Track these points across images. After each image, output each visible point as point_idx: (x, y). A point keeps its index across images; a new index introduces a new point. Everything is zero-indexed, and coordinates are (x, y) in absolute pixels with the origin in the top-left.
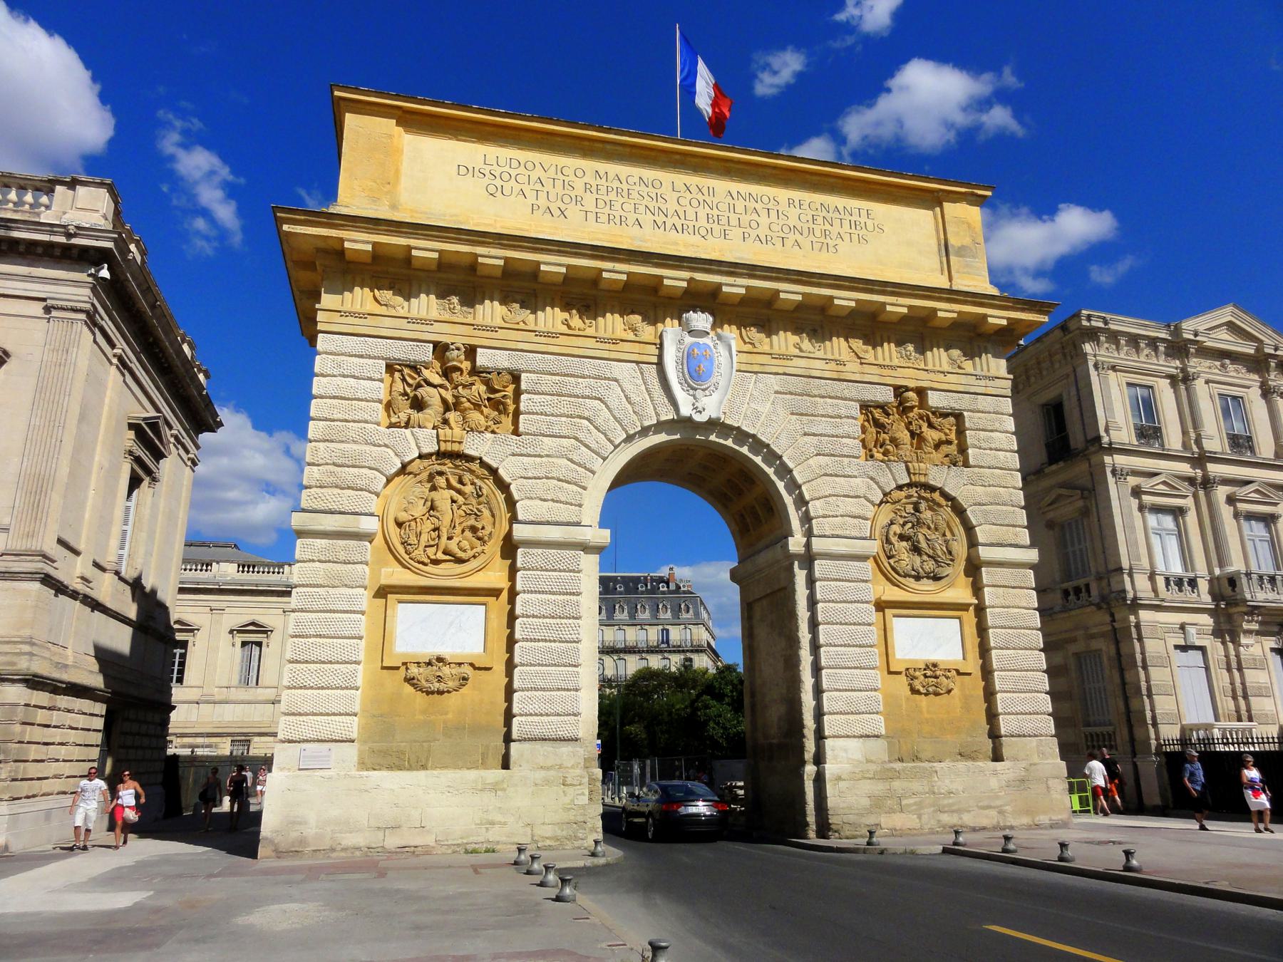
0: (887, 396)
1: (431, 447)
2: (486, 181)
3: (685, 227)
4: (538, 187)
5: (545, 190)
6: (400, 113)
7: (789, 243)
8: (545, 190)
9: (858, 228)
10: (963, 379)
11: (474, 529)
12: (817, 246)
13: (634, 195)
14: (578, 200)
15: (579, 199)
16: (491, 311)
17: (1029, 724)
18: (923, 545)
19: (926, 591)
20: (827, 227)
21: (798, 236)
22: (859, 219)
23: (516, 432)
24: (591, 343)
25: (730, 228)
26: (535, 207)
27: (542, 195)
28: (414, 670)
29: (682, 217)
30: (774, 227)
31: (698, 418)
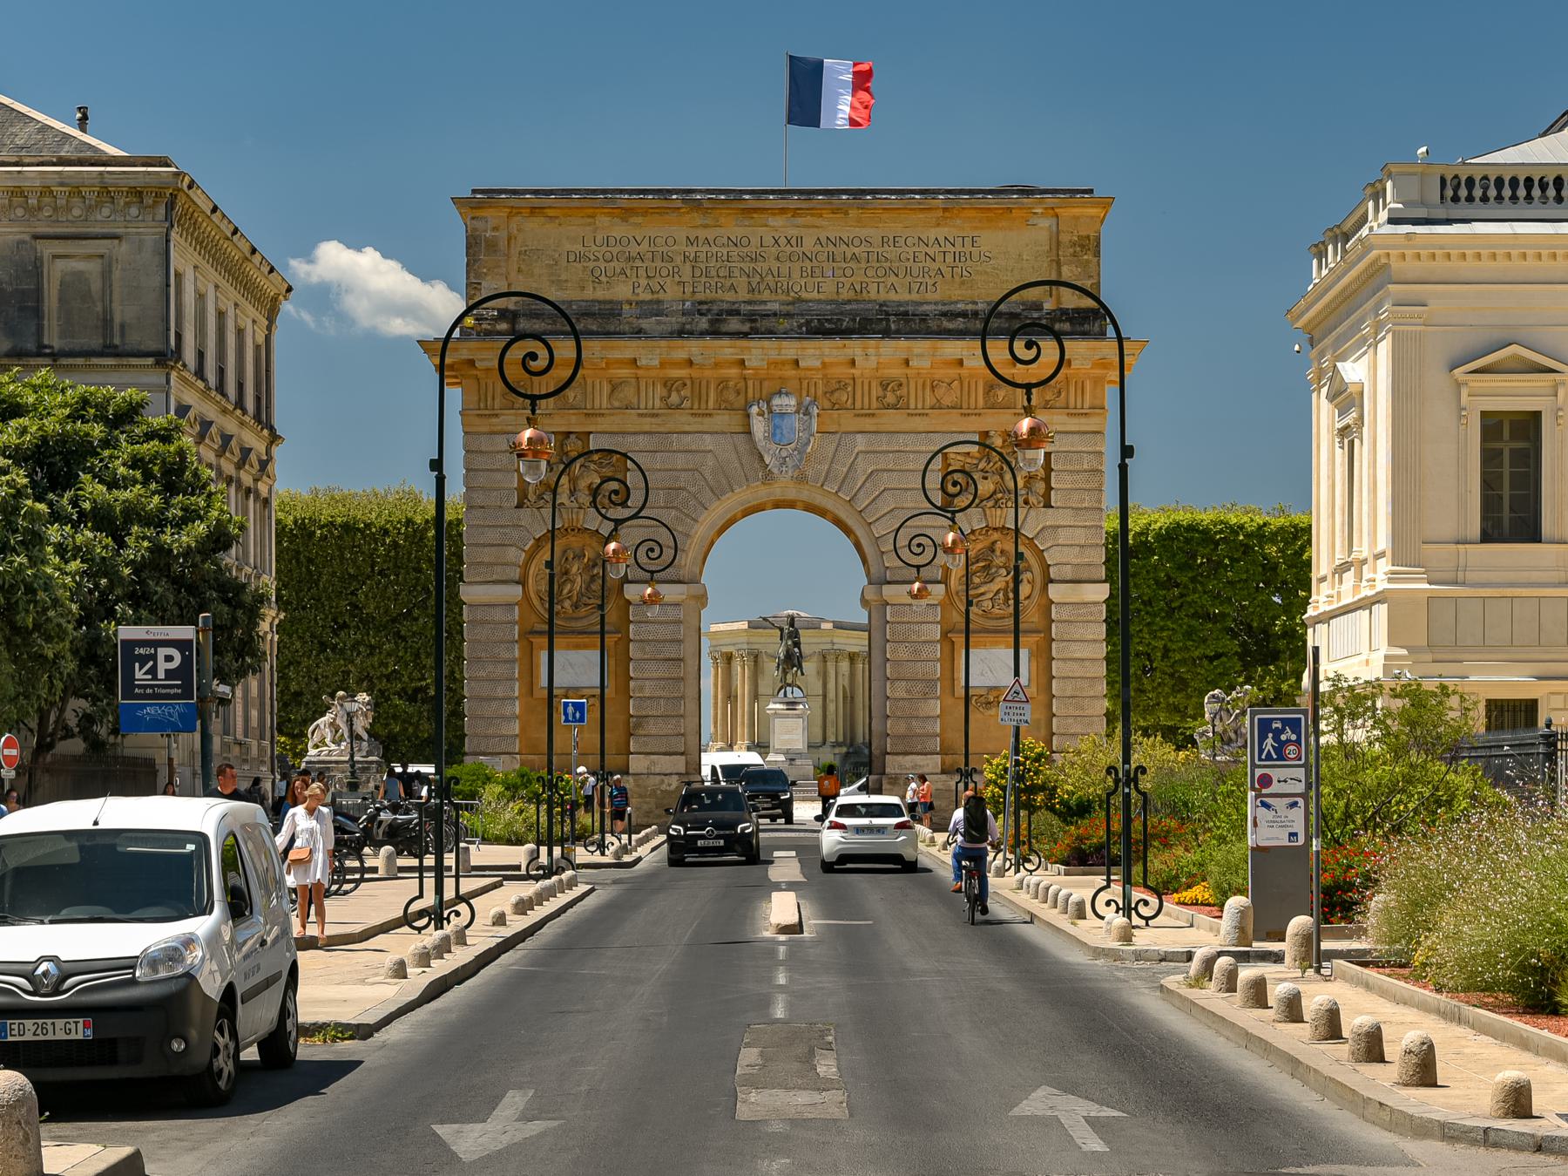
2: (591, 265)
3: (779, 284)
4: (638, 263)
5: (644, 265)
6: (508, 210)
8: (644, 265)
9: (963, 259)
12: (915, 287)
15: (676, 270)
20: (929, 262)
21: (893, 279)
22: (964, 249)
25: (823, 280)
26: (636, 285)
27: (642, 272)
29: (776, 274)
30: (870, 273)
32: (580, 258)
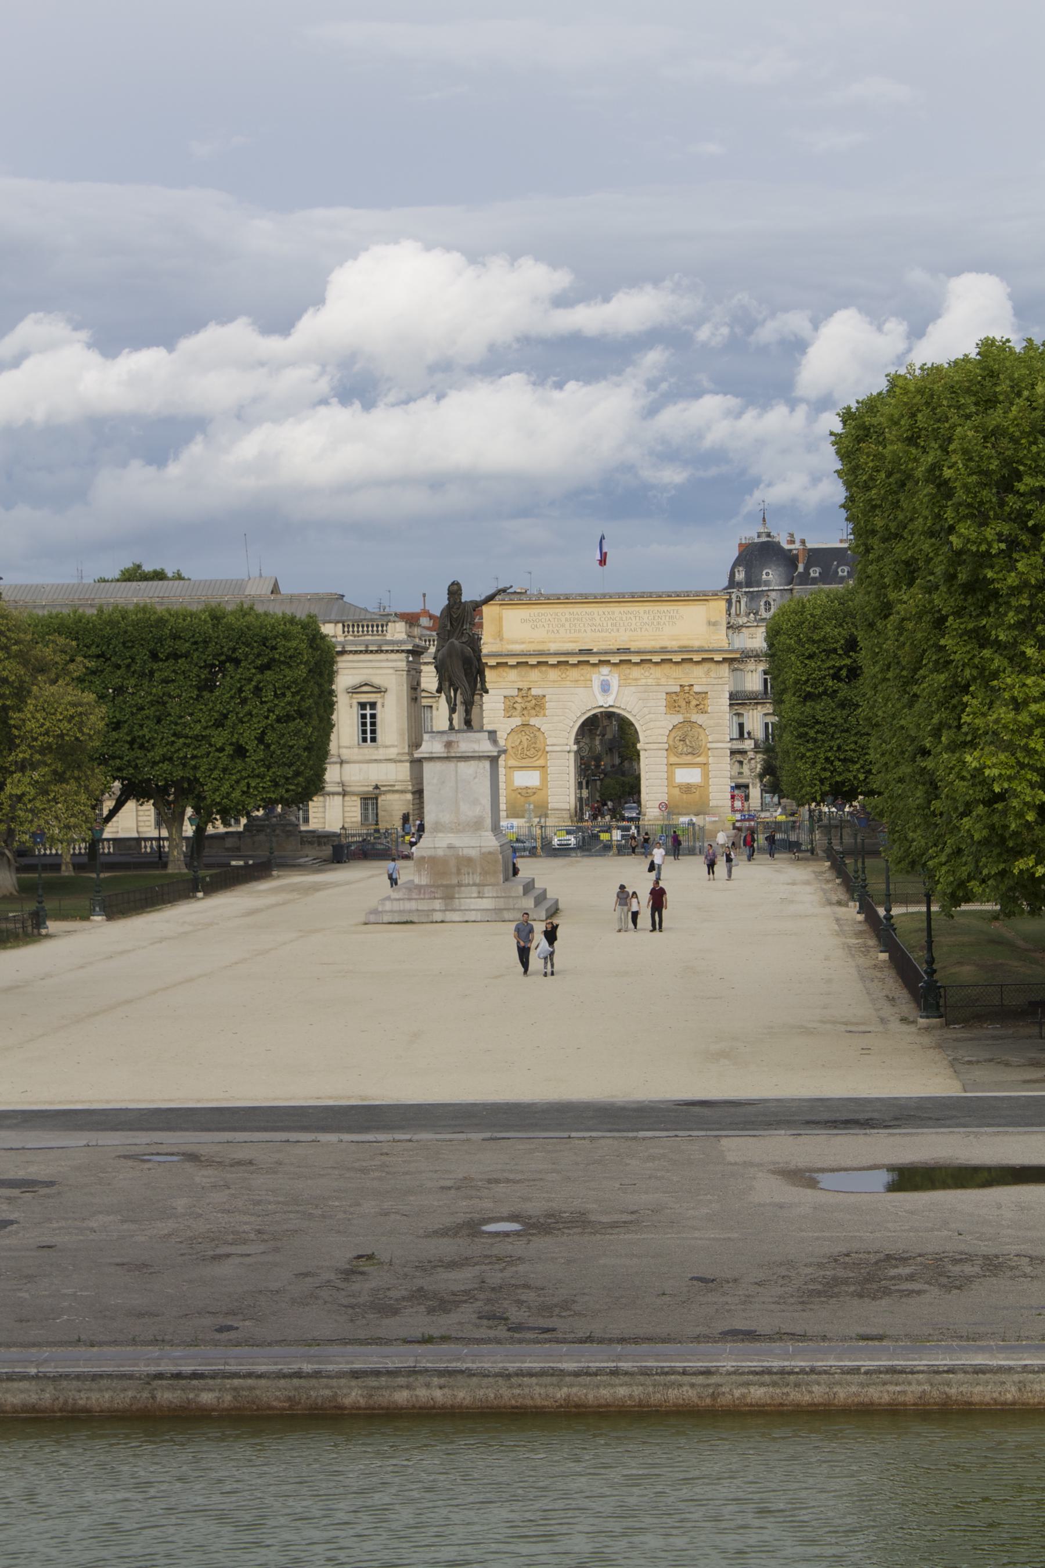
0: (677, 689)
1: (520, 724)
7: (643, 630)
10: (709, 680)
11: (534, 748)
13: (584, 620)
14: (563, 626)
16: (535, 674)
17: (720, 803)
18: (688, 743)
19: (689, 759)
23: (544, 715)
24: (568, 682)
28: (520, 791)
30: (638, 624)
31: (605, 706)
32: (525, 621)
